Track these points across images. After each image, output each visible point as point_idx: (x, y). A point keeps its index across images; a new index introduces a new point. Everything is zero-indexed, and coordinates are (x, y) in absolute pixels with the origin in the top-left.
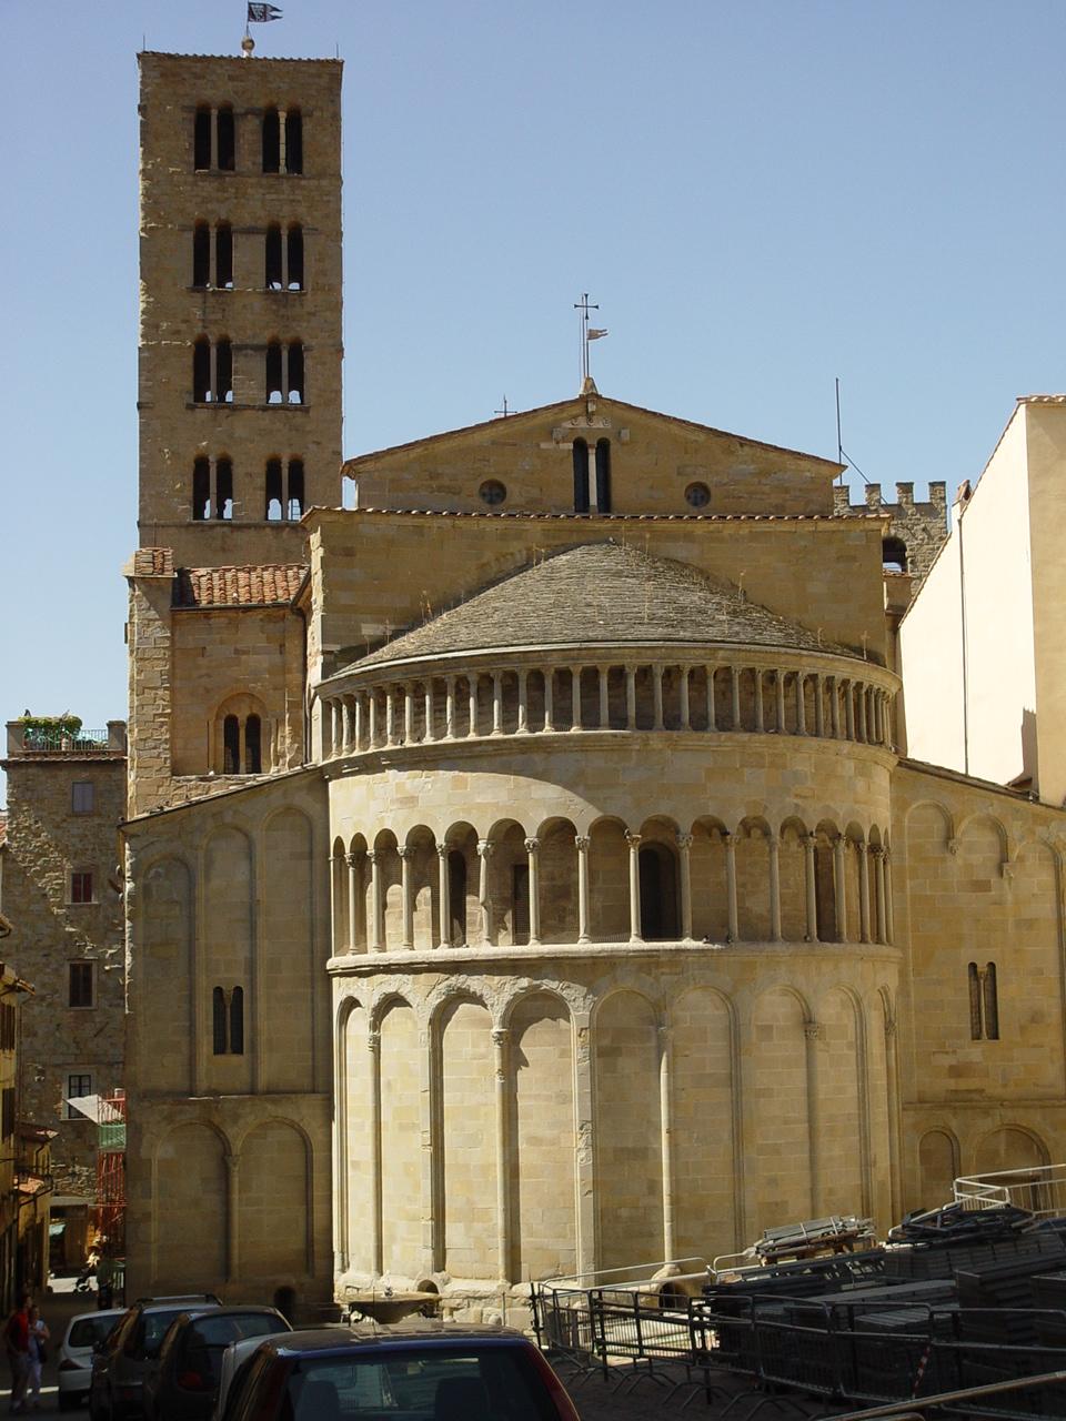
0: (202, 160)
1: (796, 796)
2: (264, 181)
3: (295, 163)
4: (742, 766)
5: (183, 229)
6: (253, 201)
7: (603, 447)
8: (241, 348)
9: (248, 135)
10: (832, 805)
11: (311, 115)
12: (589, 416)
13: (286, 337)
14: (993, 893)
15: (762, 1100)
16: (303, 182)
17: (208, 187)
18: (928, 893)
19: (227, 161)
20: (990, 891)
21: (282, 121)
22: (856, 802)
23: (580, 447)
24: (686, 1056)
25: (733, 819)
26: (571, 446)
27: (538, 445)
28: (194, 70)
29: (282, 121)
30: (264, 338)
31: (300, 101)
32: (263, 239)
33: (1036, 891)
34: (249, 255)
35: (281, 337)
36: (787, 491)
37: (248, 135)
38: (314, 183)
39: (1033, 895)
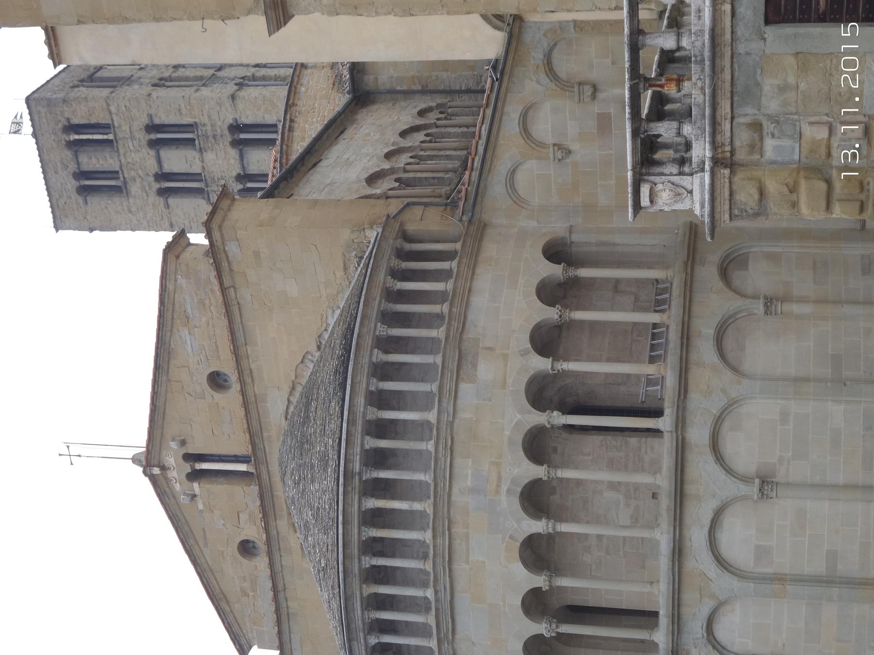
0: (117, 190)
1: (497, 492)
2: (121, 151)
3: (104, 127)
4: (467, 562)
5: (167, 206)
6: (137, 159)
7: (190, 458)
8: (243, 168)
9: (92, 161)
10: (507, 433)
11: (68, 120)
12: (163, 468)
13: (229, 138)
14: (612, 110)
15: (839, 567)
16: (116, 124)
17: (135, 188)
18: (613, 182)
19: (113, 174)
20: (609, 114)
21: (77, 137)
22: (504, 385)
23: (195, 475)
24: (784, 645)
25: (527, 580)
26: (196, 485)
27: (201, 511)
28: (58, 196)
29: (77, 137)
30: (233, 153)
31: (60, 126)
32: (163, 153)
33: (608, 61)
34: (176, 160)
35: (230, 139)
36: (202, 303)
37: (92, 161)
38: (115, 118)
39: (613, 63)
